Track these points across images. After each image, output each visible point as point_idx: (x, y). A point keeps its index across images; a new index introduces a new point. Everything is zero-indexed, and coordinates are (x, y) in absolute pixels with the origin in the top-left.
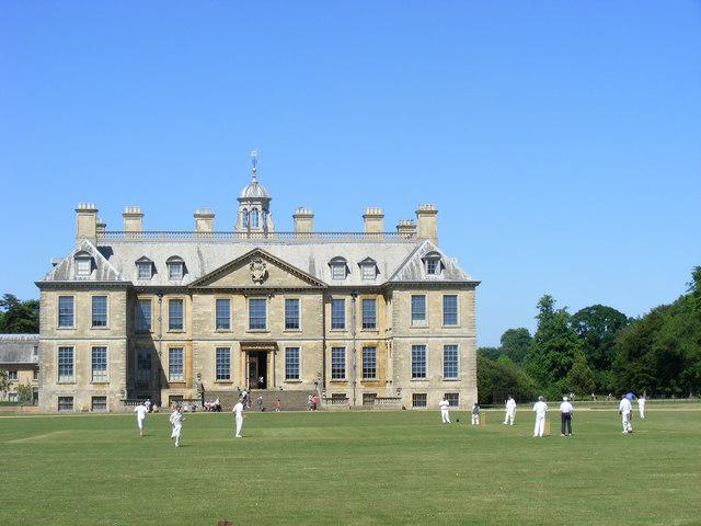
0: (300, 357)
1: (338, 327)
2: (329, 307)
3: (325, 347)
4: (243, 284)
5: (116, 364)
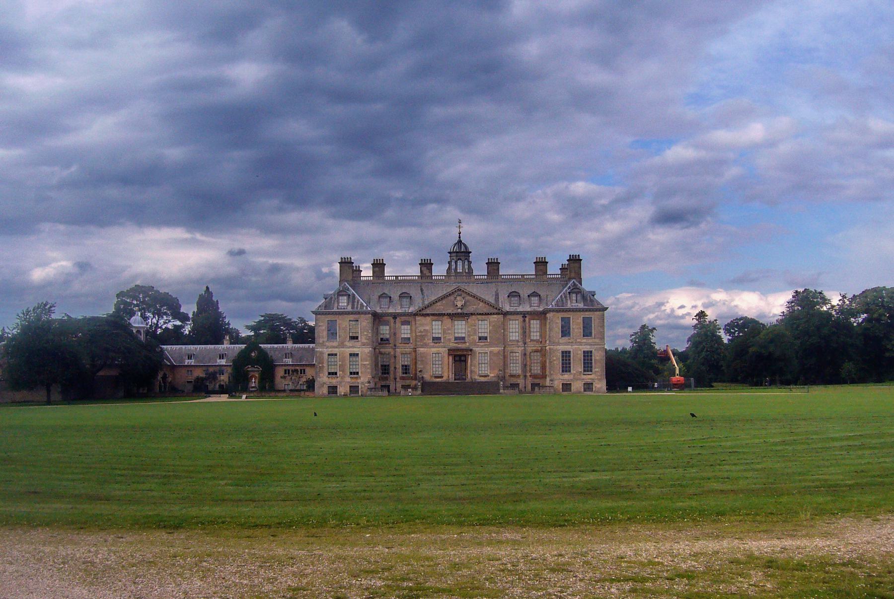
4: (449, 311)
5: (365, 365)
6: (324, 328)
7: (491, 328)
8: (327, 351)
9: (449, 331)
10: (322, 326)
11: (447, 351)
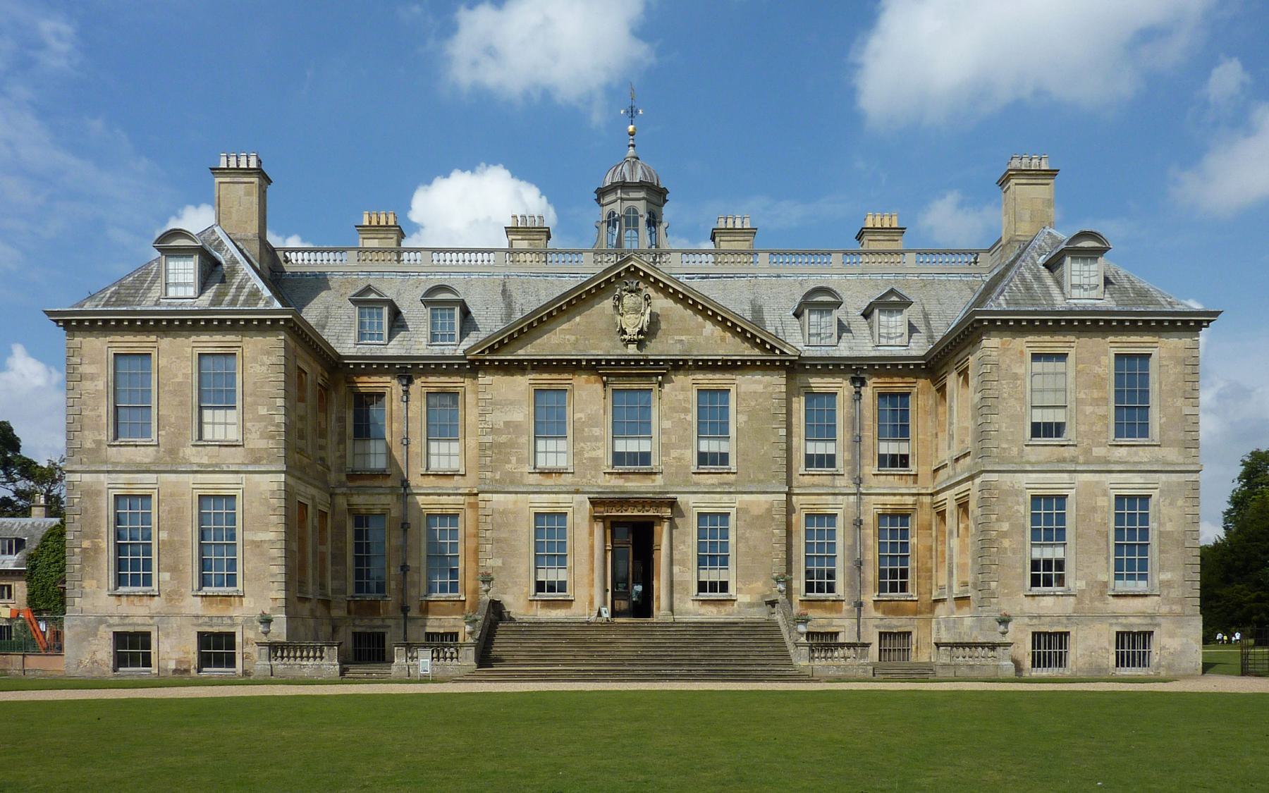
0: (732, 539)
1: (820, 465)
2: (799, 404)
3: (790, 509)
6: (100, 384)
8: (108, 485)
9: (596, 431)
10: (93, 377)
11: (588, 504)
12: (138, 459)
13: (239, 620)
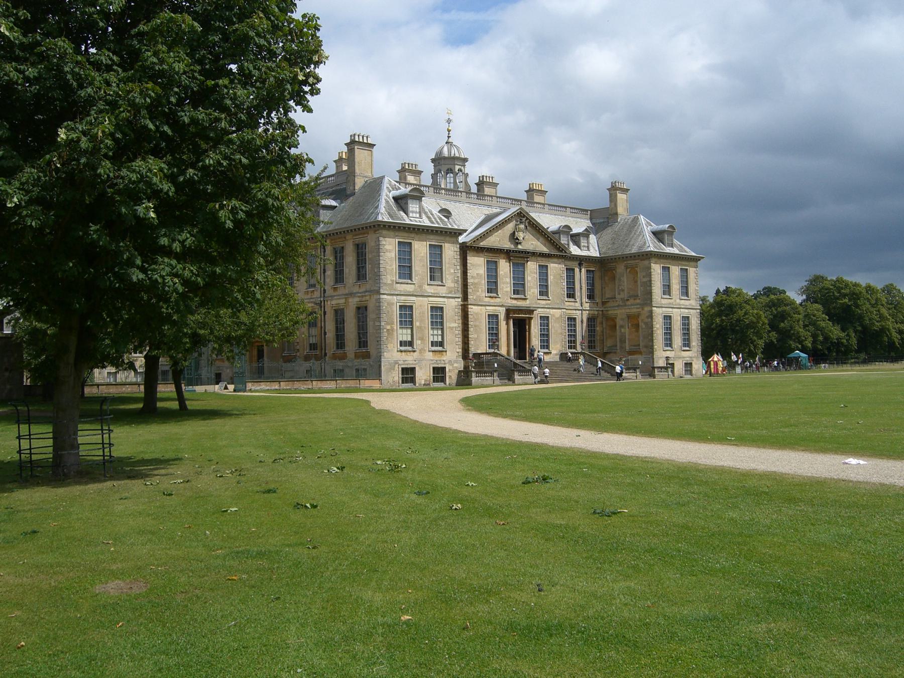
5: (451, 328)
7: (552, 277)
12: (408, 290)
13: (447, 362)
